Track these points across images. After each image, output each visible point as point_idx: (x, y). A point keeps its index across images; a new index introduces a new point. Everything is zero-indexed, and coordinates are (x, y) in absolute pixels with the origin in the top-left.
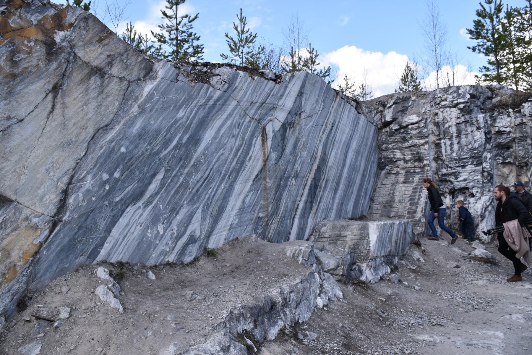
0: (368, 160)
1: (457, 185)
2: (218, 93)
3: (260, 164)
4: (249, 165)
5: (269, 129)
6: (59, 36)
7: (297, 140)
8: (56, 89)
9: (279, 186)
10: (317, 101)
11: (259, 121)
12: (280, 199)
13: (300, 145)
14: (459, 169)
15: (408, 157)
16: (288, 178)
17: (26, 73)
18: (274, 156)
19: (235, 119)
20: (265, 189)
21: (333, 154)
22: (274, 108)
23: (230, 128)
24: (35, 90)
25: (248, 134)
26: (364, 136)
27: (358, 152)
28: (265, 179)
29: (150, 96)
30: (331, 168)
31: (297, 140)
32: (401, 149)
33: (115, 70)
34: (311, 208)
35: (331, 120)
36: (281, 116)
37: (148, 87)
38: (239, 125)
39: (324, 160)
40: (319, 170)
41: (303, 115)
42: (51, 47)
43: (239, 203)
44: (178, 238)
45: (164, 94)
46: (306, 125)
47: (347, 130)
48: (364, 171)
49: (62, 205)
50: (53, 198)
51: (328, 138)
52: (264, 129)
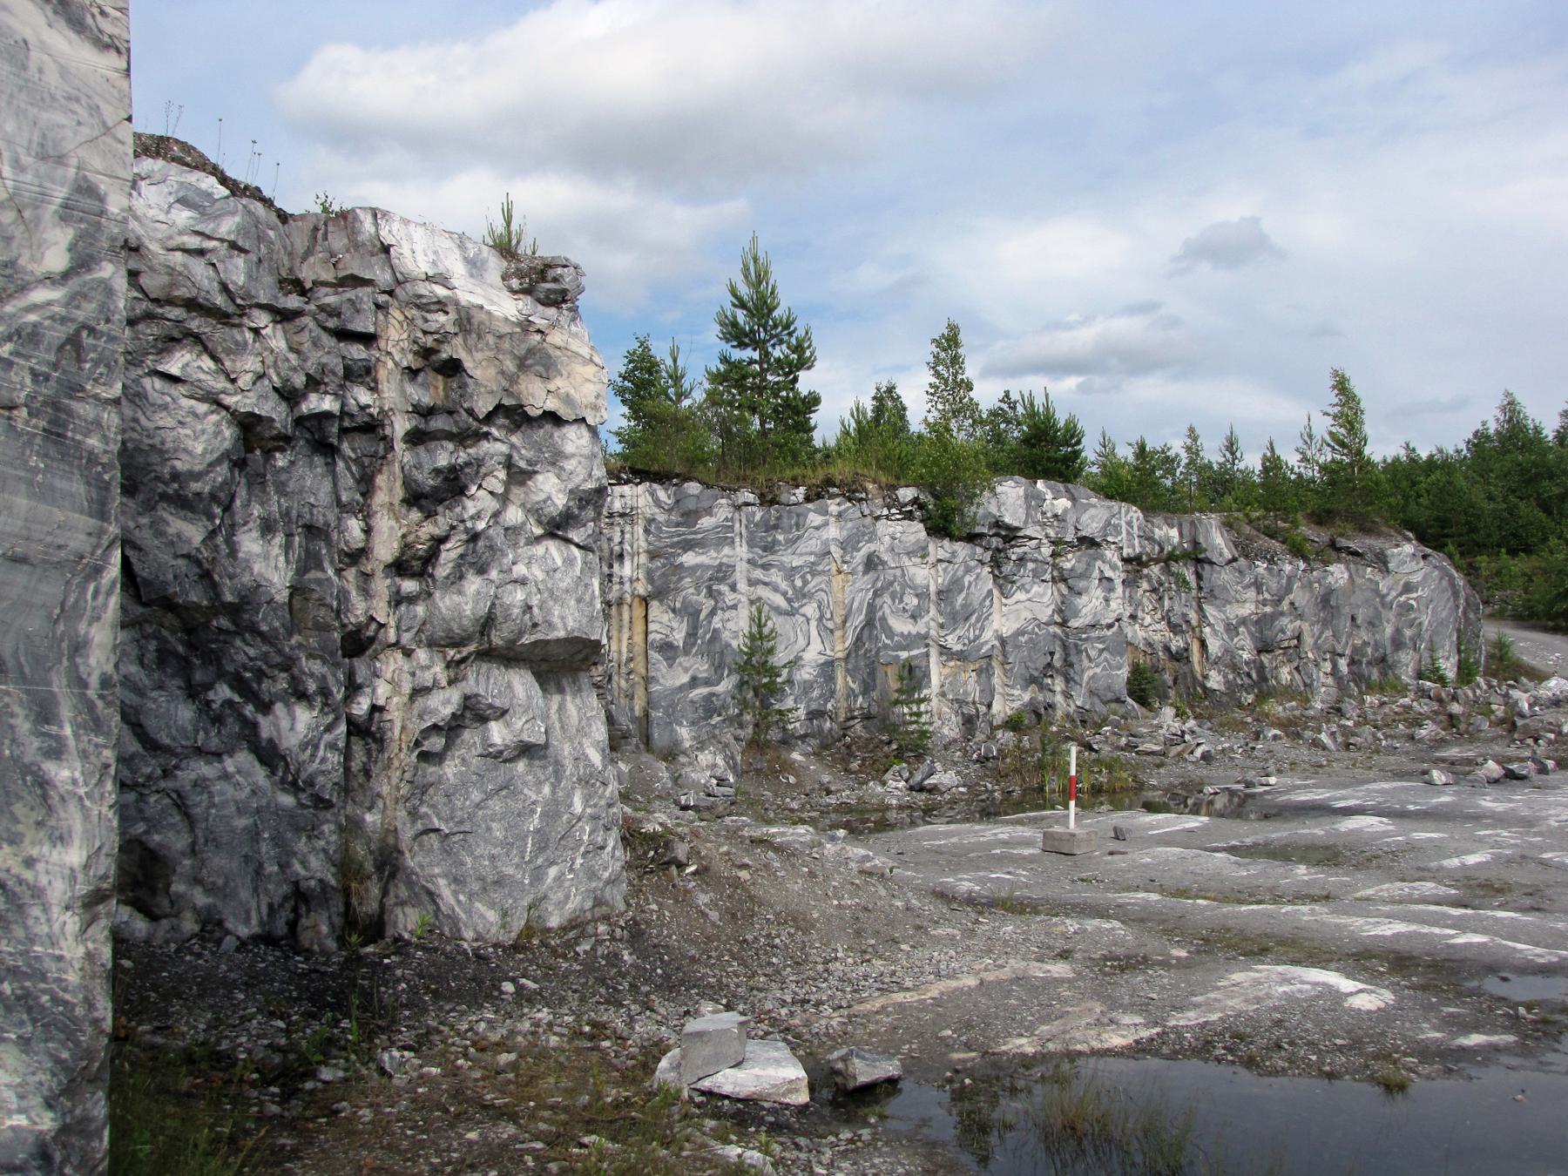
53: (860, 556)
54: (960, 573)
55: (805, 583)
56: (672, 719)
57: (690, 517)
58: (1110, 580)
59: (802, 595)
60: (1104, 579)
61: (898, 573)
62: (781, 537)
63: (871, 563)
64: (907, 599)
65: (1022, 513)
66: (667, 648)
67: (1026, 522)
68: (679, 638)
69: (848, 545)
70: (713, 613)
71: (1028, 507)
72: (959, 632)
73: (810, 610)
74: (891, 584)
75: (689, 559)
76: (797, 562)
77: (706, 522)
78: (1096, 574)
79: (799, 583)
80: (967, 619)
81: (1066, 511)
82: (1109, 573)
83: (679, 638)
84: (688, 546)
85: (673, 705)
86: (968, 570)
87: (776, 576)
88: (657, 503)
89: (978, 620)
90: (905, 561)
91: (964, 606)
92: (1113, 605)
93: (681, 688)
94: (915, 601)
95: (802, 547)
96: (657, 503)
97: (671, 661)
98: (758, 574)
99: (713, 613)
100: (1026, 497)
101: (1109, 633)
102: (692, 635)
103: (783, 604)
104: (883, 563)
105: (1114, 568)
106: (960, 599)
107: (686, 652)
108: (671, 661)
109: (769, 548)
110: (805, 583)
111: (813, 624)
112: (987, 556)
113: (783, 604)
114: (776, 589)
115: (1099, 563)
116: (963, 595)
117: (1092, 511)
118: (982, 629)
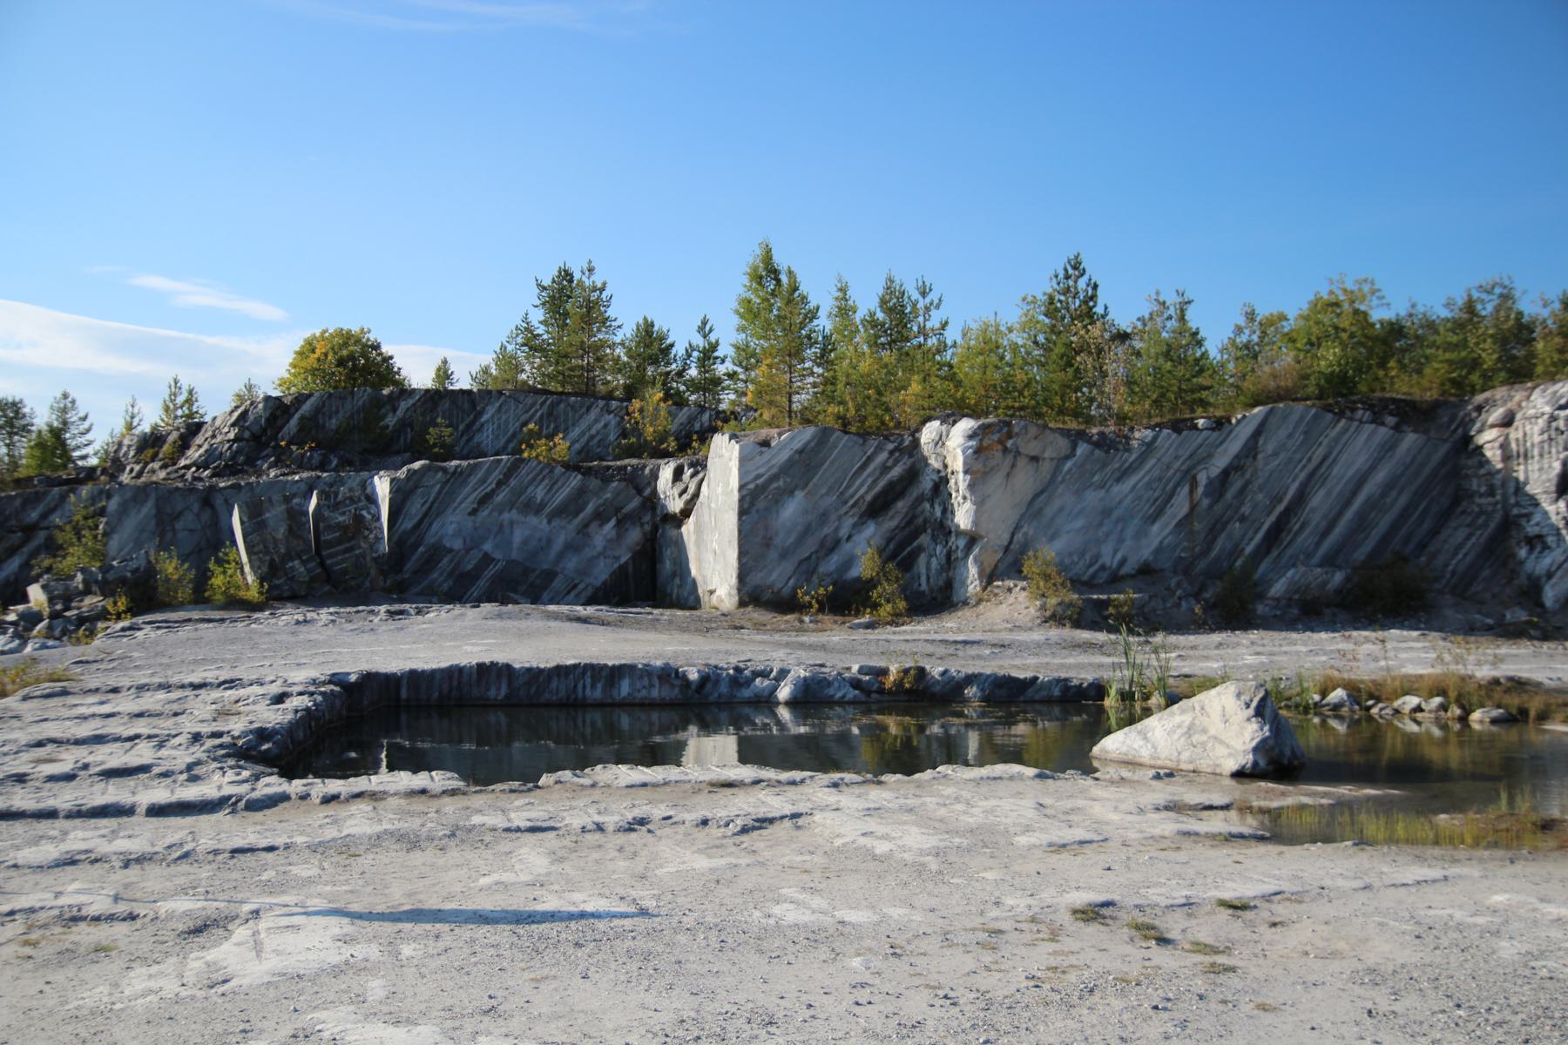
1: (1531, 530)
2: (1134, 456)
3: (1185, 510)
4: (1169, 511)
5: (1202, 478)
6: (1009, 444)
7: (1248, 483)
9: (1212, 530)
10: (1290, 436)
11: (1188, 471)
12: (1214, 540)
13: (1256, 485)
14: (1531, 509)
15: (1483, 489)
16: (1227, 522)
18: (1206, 502)
19: (1156, 473)
21: (1322, 492)
22: (1210, 456)
23: (1149, 484)
24: (997, 479)
26: (1412, 463)
27: (1389, 486)
30: (1313, 510)
31: (1248, 483)
32: (1479, 477)
33: (1046, 455)
34: (1268, 552)
35: (1321, 452)
36: (1220, 462)
37: (1069, 464)
38: (1160, 479)
39: (1301, 498)
41: (1260, 456)
42: (1005, 450)
43: (1156, 543)
44: (1091, 565)
46: (1266, 465)
49: (1010, 542)
50: (1006, 537)
52: (1194, 478)
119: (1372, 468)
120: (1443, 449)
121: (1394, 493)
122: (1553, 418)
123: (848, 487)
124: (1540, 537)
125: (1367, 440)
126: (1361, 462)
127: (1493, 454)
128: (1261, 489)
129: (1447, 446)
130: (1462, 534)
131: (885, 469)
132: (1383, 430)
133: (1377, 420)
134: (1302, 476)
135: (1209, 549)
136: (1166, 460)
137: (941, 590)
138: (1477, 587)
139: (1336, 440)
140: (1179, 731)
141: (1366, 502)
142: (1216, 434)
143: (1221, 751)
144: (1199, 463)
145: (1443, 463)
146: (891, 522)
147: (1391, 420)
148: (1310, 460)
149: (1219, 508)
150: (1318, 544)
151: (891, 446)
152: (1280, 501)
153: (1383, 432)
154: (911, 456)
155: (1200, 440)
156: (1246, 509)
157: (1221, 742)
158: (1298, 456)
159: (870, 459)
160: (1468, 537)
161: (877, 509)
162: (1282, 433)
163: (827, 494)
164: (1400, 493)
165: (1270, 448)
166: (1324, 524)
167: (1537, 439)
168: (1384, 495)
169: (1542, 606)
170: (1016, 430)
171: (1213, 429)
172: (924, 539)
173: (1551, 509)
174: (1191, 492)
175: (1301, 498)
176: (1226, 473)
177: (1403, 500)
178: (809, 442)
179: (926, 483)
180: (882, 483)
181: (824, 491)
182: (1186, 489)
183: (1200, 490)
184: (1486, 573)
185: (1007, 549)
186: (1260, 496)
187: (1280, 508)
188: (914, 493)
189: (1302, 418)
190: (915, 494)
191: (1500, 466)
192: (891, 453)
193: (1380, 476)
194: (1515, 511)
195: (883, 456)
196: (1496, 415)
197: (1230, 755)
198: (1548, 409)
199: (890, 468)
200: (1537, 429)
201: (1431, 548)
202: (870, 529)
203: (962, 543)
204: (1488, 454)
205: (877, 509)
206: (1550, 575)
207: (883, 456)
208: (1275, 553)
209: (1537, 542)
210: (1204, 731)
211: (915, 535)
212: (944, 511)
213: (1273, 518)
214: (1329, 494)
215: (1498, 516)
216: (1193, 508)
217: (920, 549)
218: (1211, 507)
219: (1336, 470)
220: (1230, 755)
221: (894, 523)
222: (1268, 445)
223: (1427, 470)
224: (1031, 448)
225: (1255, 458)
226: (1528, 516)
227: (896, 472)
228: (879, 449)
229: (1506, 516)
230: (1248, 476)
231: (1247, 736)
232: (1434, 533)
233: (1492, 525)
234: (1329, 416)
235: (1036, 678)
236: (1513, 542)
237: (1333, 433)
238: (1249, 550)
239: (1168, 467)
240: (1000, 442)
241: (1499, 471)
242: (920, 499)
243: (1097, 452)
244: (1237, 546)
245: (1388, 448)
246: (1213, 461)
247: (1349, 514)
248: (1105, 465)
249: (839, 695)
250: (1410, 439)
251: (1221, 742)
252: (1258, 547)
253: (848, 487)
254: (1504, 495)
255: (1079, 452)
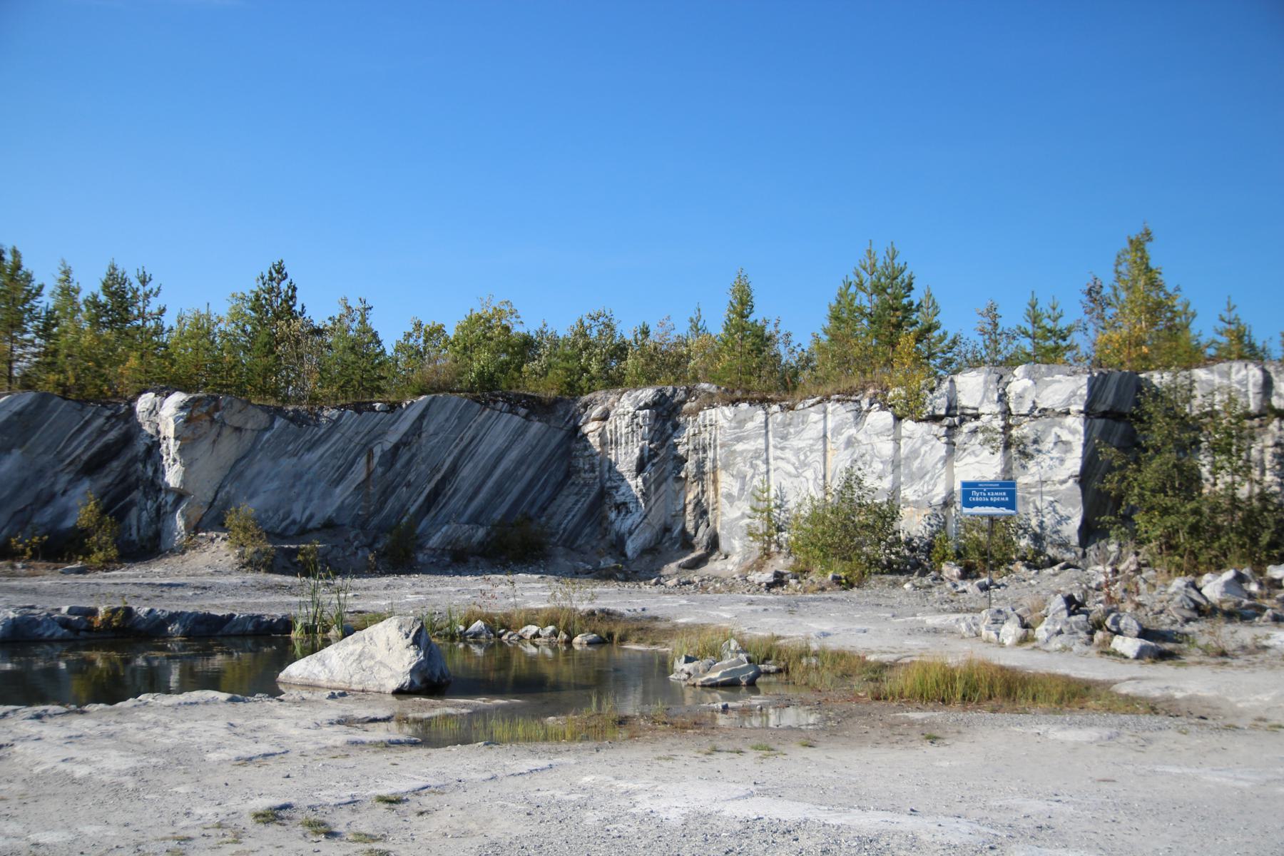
0: (543, 469)
1: (619, 499)
3: (363, 476)
4: (350, 477)
5: (378, 451)
6: (216, 415)
7: (414, 456)
8: (214, 442)
9: (384, 492)
10: (447, 420)
11: (366, 445)
13: (419, 458)
15: (587, 467)
17: (200, 436)
18: (380, 470)
20: (368, 494)
21: (471, 465)
22: (384, 433)
23: (334, 453)
24: (204, 446)
25: (352, 455)
27: (520, 462)
28: (368, 487)
29: (268, 440)
30: (463, 479)
33: (249, 426)
35: (470, 433)
36: (392, 438)
37: (267, 435)
38: (343, 450)
39: (454, 470)
40: (444, 480)
41: (424, 435)
42: (213, 421)
43: (338, 503)
44: (283, 520)
45: (279, 436)
46: (427, 442)
47: (500, 441)
48: (532, 480)
49: (214, 499)
50: (211, 494)
51: (463, 451)
52: (371, 450)
53: (842, 439)
54: (917, 445)
55: (806, 457)
56: (731, 536)
57: (741, 423)
58: (1066, 443)
59: (804, 464)
60: (1059, 441)
61: (869, 447)
62: (792, 430)
63: (850, 443)
64: (874, 465)
65: (979, 397)
66: (729, 497)
67: (982, 402)
68: (735, 491)
69: (838, 430)
70: (753, 477)
71: (986, 390)
72: (915, 487)
73: (809, 474)
74: (863, 456)
75: (739, 447)
76: (802, 444)
77: (750, 425)
78: (1052, 438)
79: (802, 457)
80: (922, 478)
81: (1025, 389)
82: (1066, 436)
83: (735, 491)
84: (739, 439)
85: (731, 528)
86: (925, 442)
87: (788, 454)
88: (725, 417)
89: (931, 479)
90: (875, 439)
91: (920, 469)
92: (1068, 464)
93: (736, 519)
94: (881, 466)
95: (806, 435)
96: (725, 417)
97: (731, 503)
98: (779, 453)
99: (753, 477)
100: (986, 382)
101: (1064, 487)
102: (742, 489)
103: (793, 471)
104: (859, 442)
105: (1073, 432)
106: (916, 464)
107: (739, 499)
108: (731, 503)
109: (784, 438)
110: (806, 457)
111: (811, 482)
112: (943, 431)
113: (793, 471)
114: (788, 462)
115: (1056, 430)
116: (919, 460)
117: (1056, 386)
118: (935, 485)
119: (508, 448)
120: (560, 435)
121: (524, 468)
122: (635, 416)
123: (65, 447)
124: (624, 504)
125: (505, 425)
126: (500, 442)
127: (594, 440)
128: (424, 461)
129: (562, 433)
130: (572, 499)
131: (101, 432)
132: (517, 418)
133: (512, 411)
134: (456, 451)
135: (381, 508)
136: (349, 434)
137: (150, 539)
138: (581, 541)
139: (482, 425)
140: (352, 658)
141: (503, 473)
142: (389, 415)
143: (385, 673)
144: (376, 438)
145: (559, 446)
146: (105, 480)
147: (523, 411)
148: (462, 439)
149: (390, 475)
150: (466, 507)
151: (108, 413)
152: (438, 471)
153: (517, 421)
154: (126, 422)
155: (376, 420)
156: (411, 477)
157: (385, 666)
158: (453, 436)
159: (87, 423)
160: (575, 504)
161: (92, 467)
162: (441, 417)
163: (45, 452)
164: (528, 468)
165: (431, 429)
166: (471, 490)
167: (624, 431)
168: (516, 469)
169: (625, 555)
170: (223, 404)
171: (387, 412)
172: (137, 495)
173: (632, 483)
174: (369, 462)
175: (454, 470)
176: (396, 447)
177: (530, 474)
178: (28, 405)
179: (140, 446)
180: (98, 445)
181: (41, 450)
182: (364, 460)
183: (376, 460)
184: (587, 530)
185: (211, 505)
186: (423, 467)
187: (439, 476)
188: (128, 455)
189: (457, 406)
190: (129, 456)
191: (598, 450)
192: (108, 418)
193: (514, 455)
194: (608, 484)
195: (101, 421)
196: (596, 411)
197: (392, 676)
198: (631, 409)
199: (107, 432)
200: (624, 424)
201: (550, 511)
202: (86, 485)
203: (171, 499)
204: (591, 440)
205: (92, 467)
206: (631, 533)
207: (101, 421)
208: (433, 513)
209: (622, 507)
210: (372, 657)
211: (128, 491)
212: (156, 471)
213: (432, 484)
214: (475, 466)
215: (597, 487)
216: (369, 475)
217: (132, 503)
218: (384, 474)
219: (480, 449)
220: (392, 676)
221: (108, 480)
222: (430, 427)
223: (548, 451)
224: (236, 420)
225: (419, 436)
226: (617, 488)
227: (112, 435)
228: (97, 414)
229: (602, 487)
230: (414, 450)
231: (406, 660)
232: (552, 498)
233: (593, 494)
234: (478, 405)
235: (232, 615)
236: (607, 507)
237: (480, 420)
238: (412, 510)
239: (350, 441)
240: (208, 413)
241: (598, 454)
242: (134, 460)
243: (292, 426)
244: (403, 506)
245: (520, 432)
246: (387, 437)
247: (490, 483)
248: (298, 437)
249: (48, 633)
250: (536, 426)
251: (385, 666)
252: (421, 507)
253: (65, 447)
254: (601, 472)
255: (276, 425)
